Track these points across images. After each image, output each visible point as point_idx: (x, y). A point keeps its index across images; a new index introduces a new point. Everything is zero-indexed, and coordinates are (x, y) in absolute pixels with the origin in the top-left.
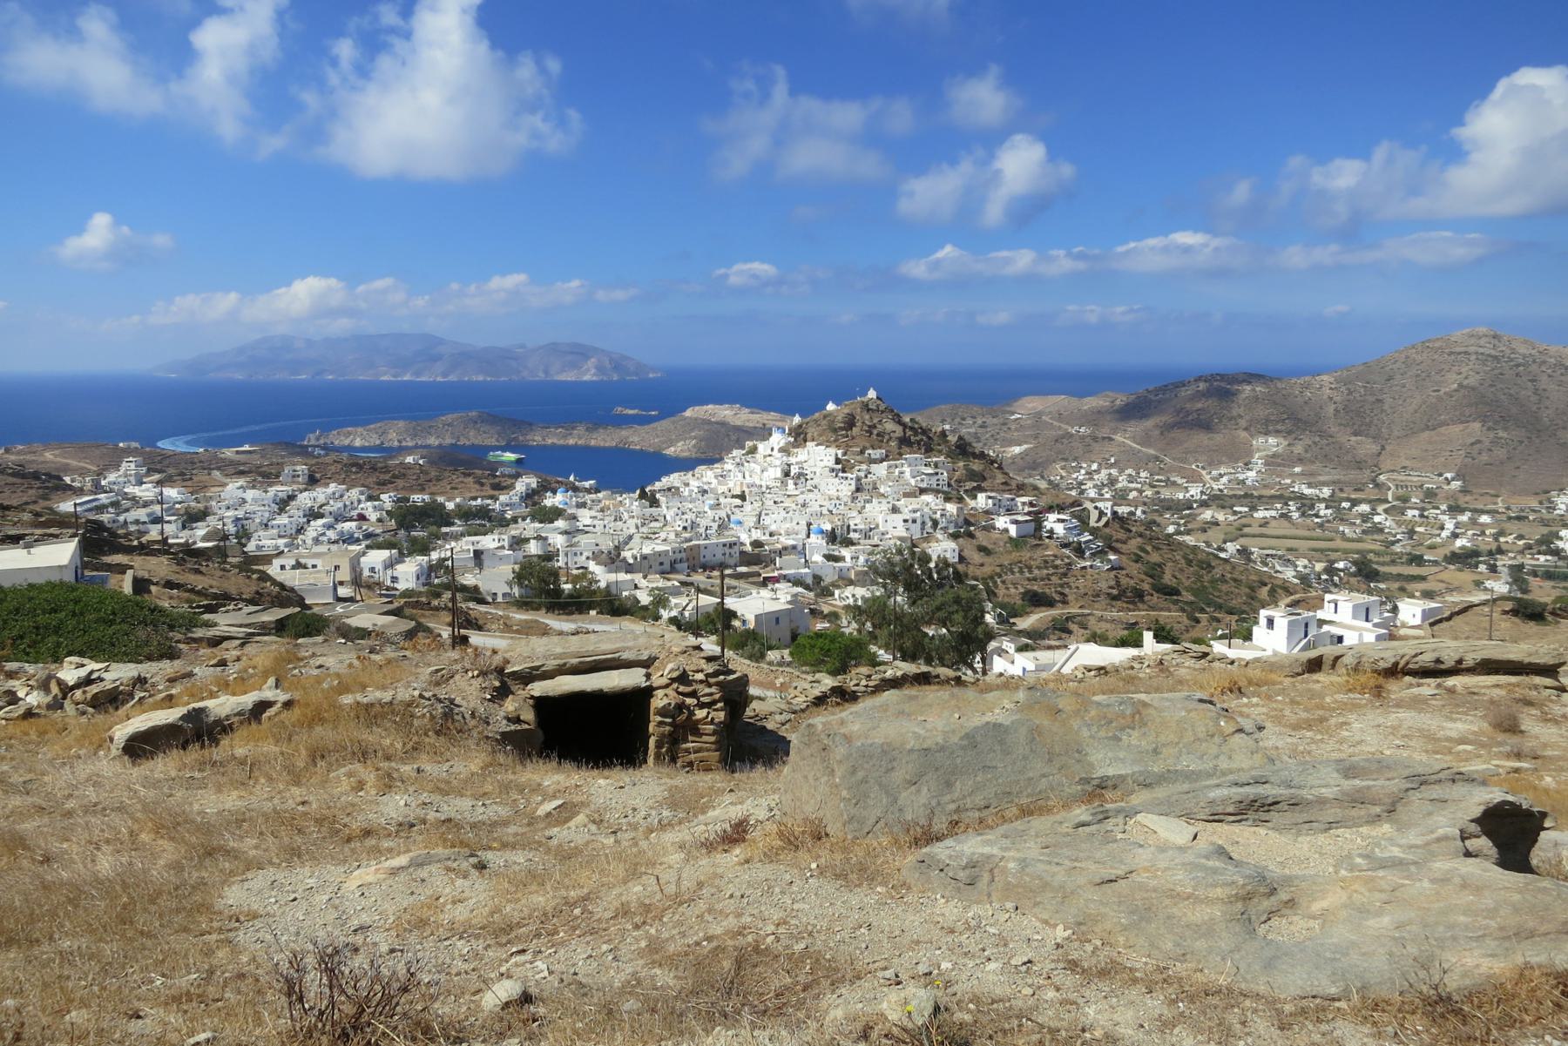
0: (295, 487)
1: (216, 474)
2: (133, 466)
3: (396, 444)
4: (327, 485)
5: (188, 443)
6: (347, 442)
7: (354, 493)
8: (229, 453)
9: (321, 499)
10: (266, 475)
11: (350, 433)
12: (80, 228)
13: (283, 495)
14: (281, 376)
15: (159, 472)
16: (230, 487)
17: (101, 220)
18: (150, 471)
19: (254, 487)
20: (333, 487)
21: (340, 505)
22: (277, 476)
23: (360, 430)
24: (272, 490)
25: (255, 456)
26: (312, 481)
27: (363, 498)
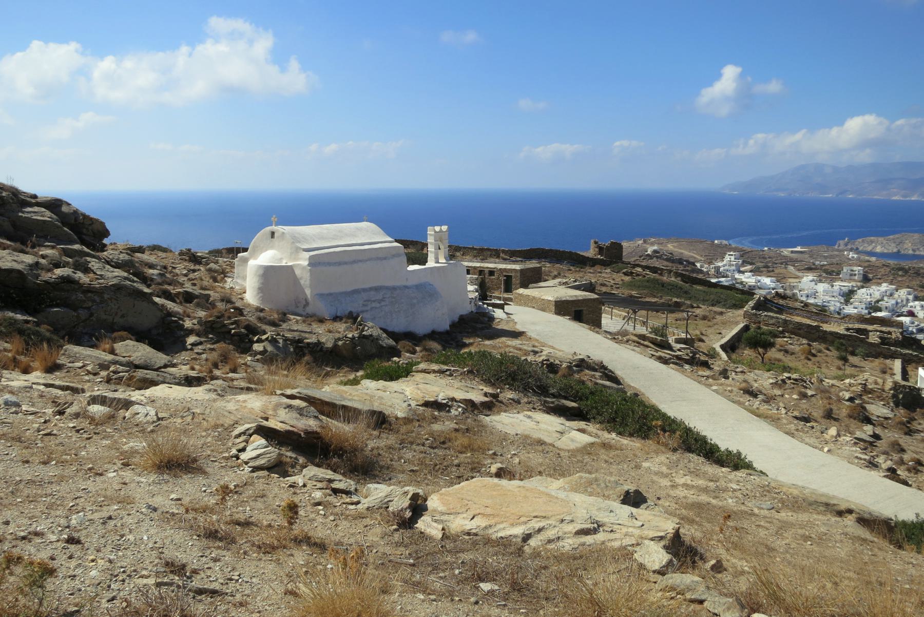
0: (854, 284)
1: (791, 268)
2: (733, 258)
3: (911, 252)
4: (879, 284)
5: (752, 242)
6: (869, 248)
7: (903, 293)
8: (786, 252)
9: (877, 295)
10: (830, 273)
11: (872, 242)
12: (719, 76)
13: (845, 289)
14: (813, 195)
15: (751, 264)
16: (805, 279)
17: (730, 72)
18: (745, 263)
19: (820, 281)
20: (885, 287)
21: (893, 302)
22: (838, 274)
23: (881, 239)
24: (837, 284)
25: (807, 256)
26: (866, 280)
27: (911, 297)
